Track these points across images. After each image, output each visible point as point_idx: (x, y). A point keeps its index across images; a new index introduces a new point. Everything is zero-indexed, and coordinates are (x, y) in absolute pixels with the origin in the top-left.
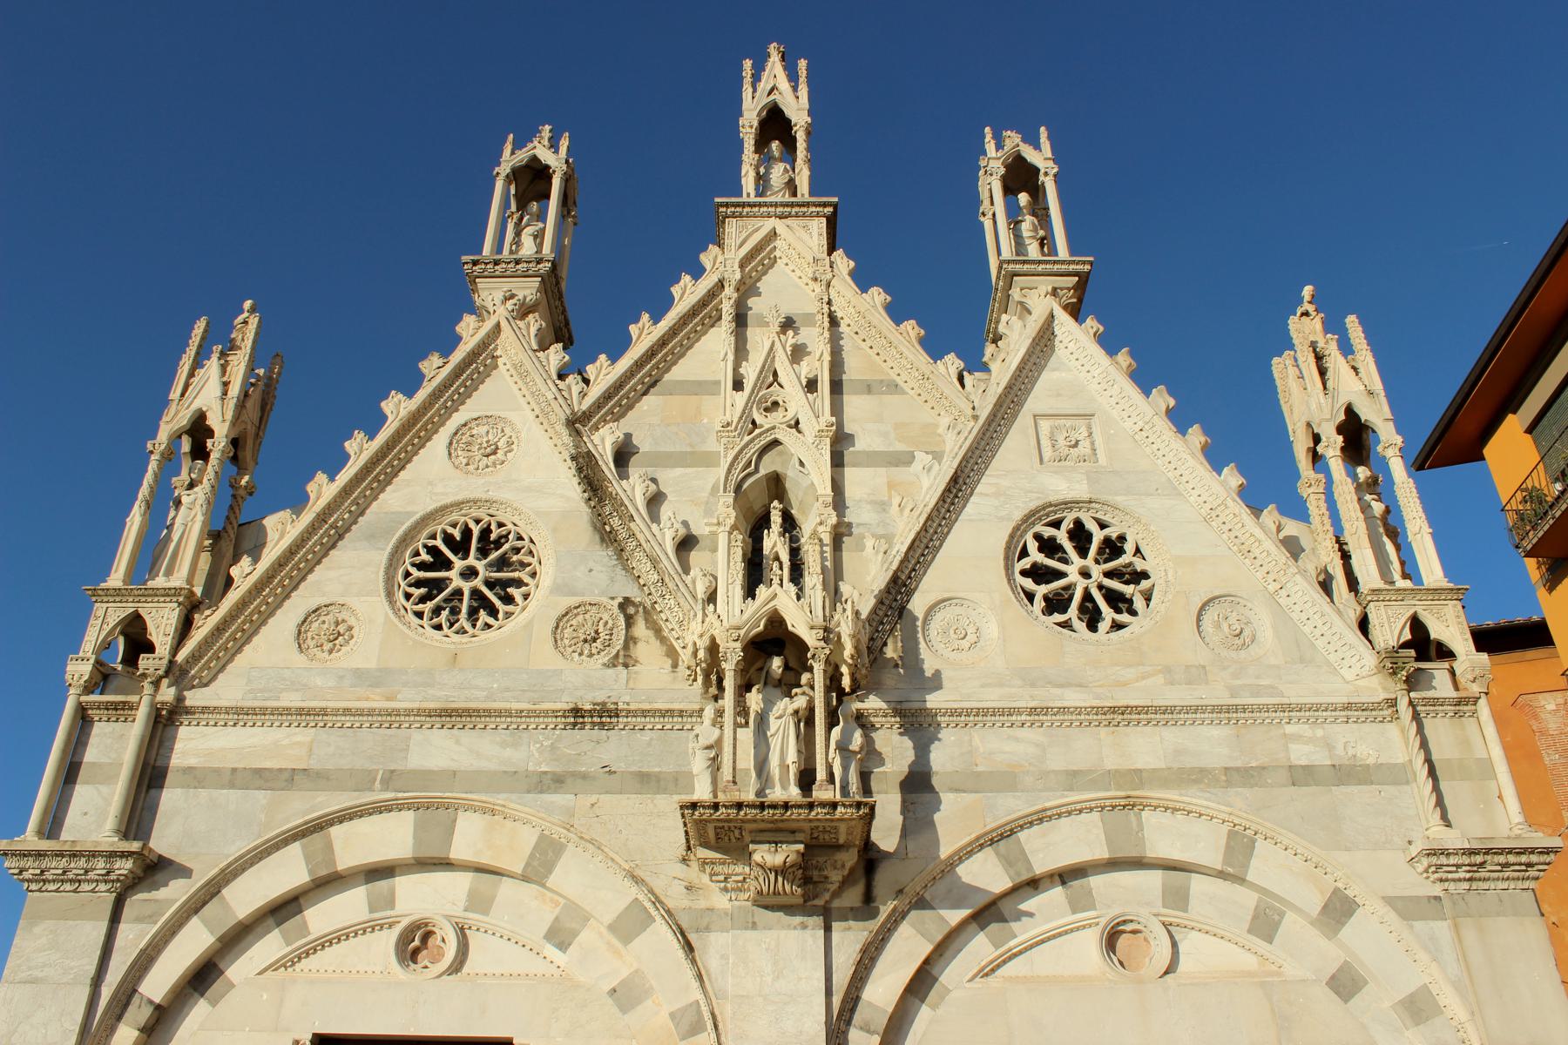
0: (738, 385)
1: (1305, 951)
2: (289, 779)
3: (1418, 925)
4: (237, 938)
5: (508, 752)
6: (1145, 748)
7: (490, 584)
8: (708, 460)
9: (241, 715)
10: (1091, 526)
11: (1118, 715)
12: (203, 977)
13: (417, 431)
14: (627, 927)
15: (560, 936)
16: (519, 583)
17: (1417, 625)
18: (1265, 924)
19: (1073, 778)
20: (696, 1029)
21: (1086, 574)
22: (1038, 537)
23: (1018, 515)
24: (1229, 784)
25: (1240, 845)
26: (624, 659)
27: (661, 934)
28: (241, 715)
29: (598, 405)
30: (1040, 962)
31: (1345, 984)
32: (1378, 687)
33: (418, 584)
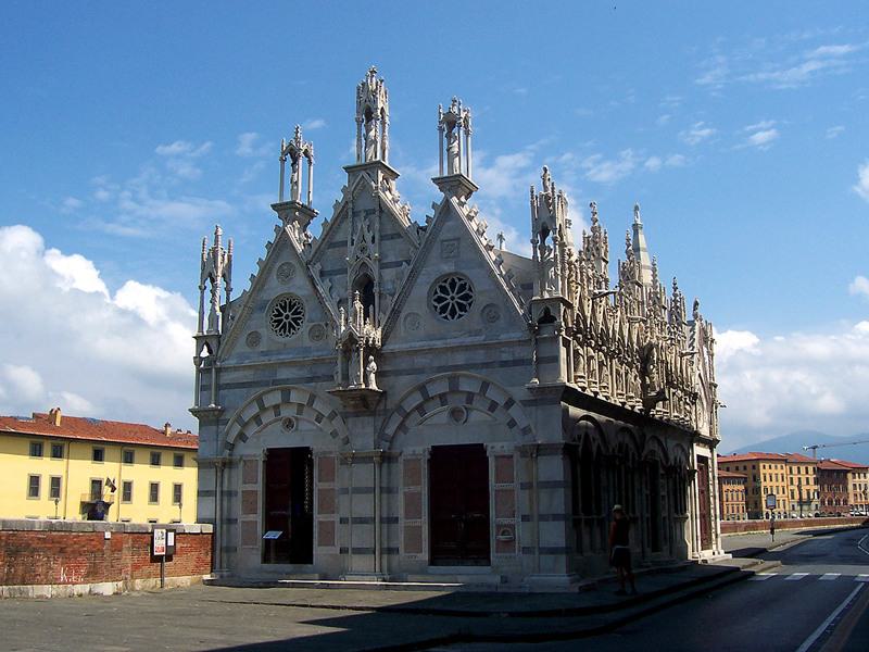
0: (353, 244)
3: (528, 409)
4: (245, 425)
5: (301, 373)
6: (460, 359)
7: (293, 319)
8: (345, 271)
9: (236, 369)
10: (457, 280)
11: (453, 349)
12: (242, 437)
15: (319, 419)
16: (300, 319)
17: (547, 311)
19: (440, 369)
20: (348, 442)
21: (453, 298)
22: (441, 287)
23: (432, 281)
24: (482, 368)
25: (485, 385)
28: (236, 369)
29: (314, 256)
30: (435, 420)
32: (526, 335)
33: (275, 321)
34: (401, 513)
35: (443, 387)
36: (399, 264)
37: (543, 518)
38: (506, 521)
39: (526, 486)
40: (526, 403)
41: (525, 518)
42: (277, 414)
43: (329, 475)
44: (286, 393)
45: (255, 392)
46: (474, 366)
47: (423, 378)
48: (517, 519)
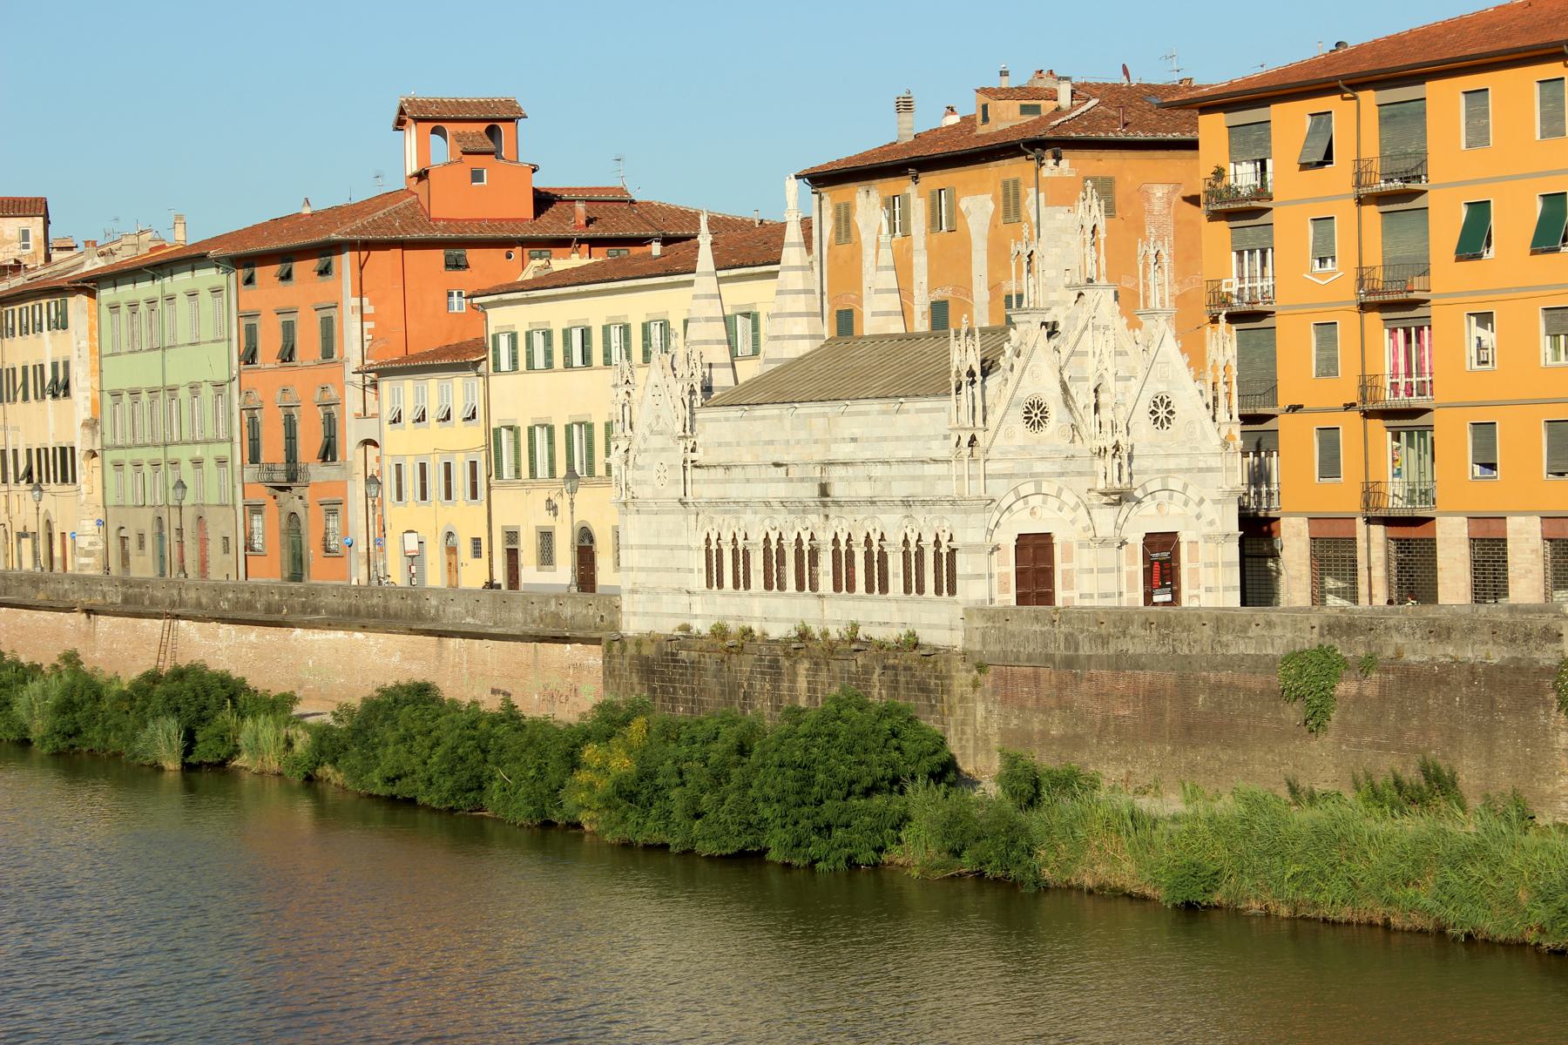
1: (1192, 509)
2: (1011, 476)
6: (1172, 464)
13: (1024, 369)
14: (1074, 509)
18: (1186, 504)
19: (1158, 471)
25: (1186, 486)
26: (1073, 441)
27: (1082, 508)
31: (1198, 517)
32: (1219, 449)
34: (1124, 590)
35: (1155, 485)
36: (1129, 379)
37: (1226, 589)
38: (1196, 592)
39: (1206, 565)
40: (1215, 502)
41: (1208, 590)
42: (1026, 503)
43: (1068, 557)
44: (1038, 485)
45: (1014, 482)
46: (1180, 470)
47: (1146, 478)
48: (1202, 589)
